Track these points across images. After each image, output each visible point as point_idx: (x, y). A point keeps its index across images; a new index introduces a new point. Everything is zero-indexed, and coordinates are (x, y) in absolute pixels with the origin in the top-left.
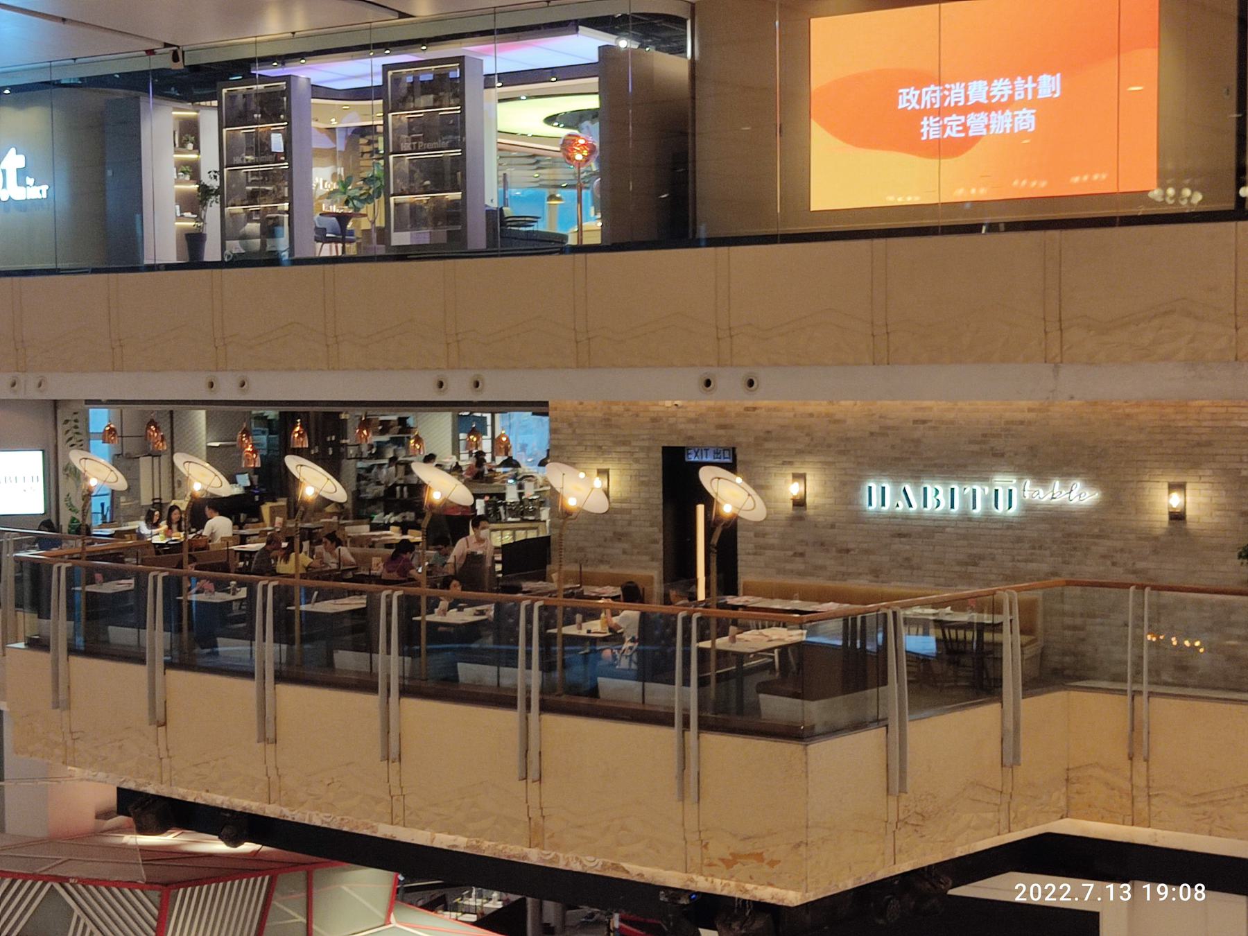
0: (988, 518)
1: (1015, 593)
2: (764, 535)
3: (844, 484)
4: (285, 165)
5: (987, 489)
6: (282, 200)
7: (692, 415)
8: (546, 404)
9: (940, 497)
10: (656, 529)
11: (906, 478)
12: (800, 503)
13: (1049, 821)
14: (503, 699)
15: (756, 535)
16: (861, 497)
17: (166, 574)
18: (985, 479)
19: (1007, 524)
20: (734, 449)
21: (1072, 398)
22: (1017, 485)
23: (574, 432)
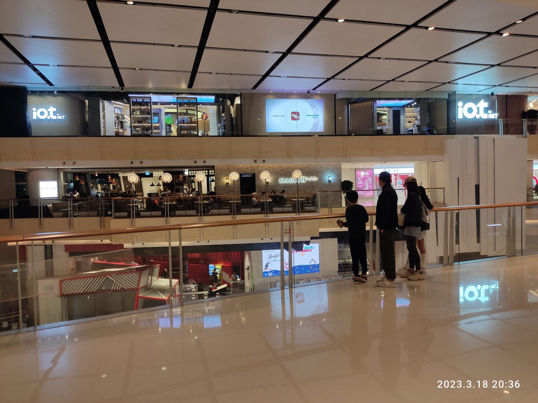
2: (261, 189)
7: (246, 168)
10: (239, 189)
15: (259, 189)
23: (221, 171)
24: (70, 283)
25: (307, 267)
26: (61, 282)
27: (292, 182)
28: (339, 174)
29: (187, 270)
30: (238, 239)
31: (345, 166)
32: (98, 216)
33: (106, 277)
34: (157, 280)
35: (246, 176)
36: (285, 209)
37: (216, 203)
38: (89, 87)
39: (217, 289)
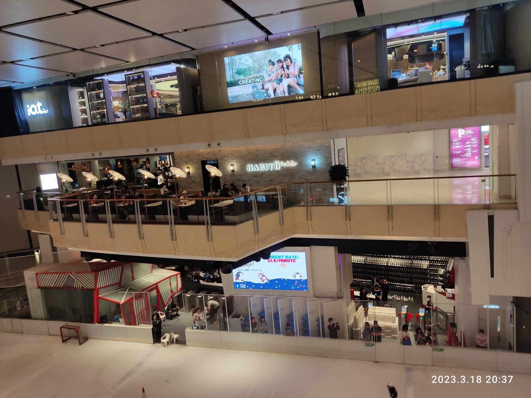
0: (274, 171)
1: (280, 187)
3: (242, 166)
4: (104, 101)
5: (273, 164)
6: (104, 109)
8: (173, 153)
9: (263, 167)
11: (256, 163)
12: (233, 171)
13: (291, 235)
14: (166, 223)
15: (224, 179)
16: (246, 168)
17: (83, 201)
18: (272, 162)
19: (278, 172)
20: (217, 160)
21: (289, 142)
22: (280, 163)
23: (180, 159)
24: (43, 277)
25: (290, 282)
28: (327, 156)
33: (68, 275)
35: (211, 163)
38: (50, 79)
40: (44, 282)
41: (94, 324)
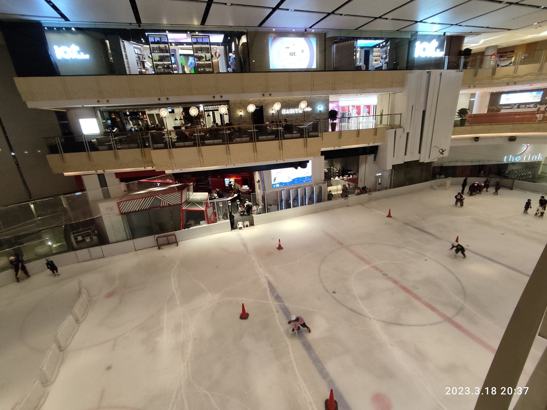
0: (298, 113)
15: (267, 119)
23: (235, 105)
26: (118, 204)
27: (292, 113)
29: (210, 184)
30: (259, 162)
31: (332, 98)
32: (138, 147)
34: (192, 194)
36: (294, 135)
37: (236, 133)
39: (235, 196)
40: (128, 207)
41: (181, 230)
